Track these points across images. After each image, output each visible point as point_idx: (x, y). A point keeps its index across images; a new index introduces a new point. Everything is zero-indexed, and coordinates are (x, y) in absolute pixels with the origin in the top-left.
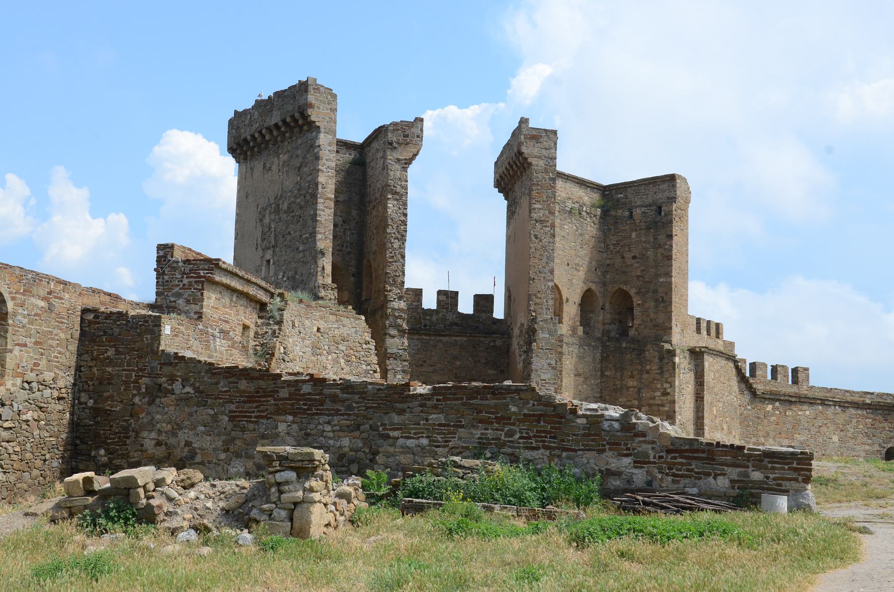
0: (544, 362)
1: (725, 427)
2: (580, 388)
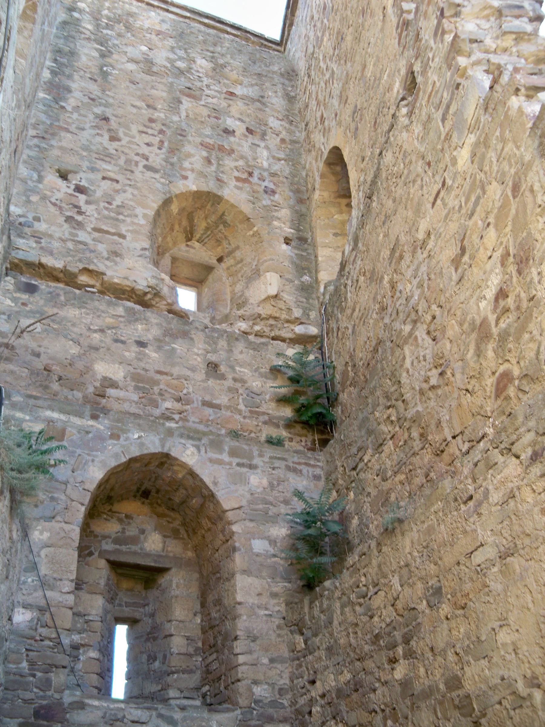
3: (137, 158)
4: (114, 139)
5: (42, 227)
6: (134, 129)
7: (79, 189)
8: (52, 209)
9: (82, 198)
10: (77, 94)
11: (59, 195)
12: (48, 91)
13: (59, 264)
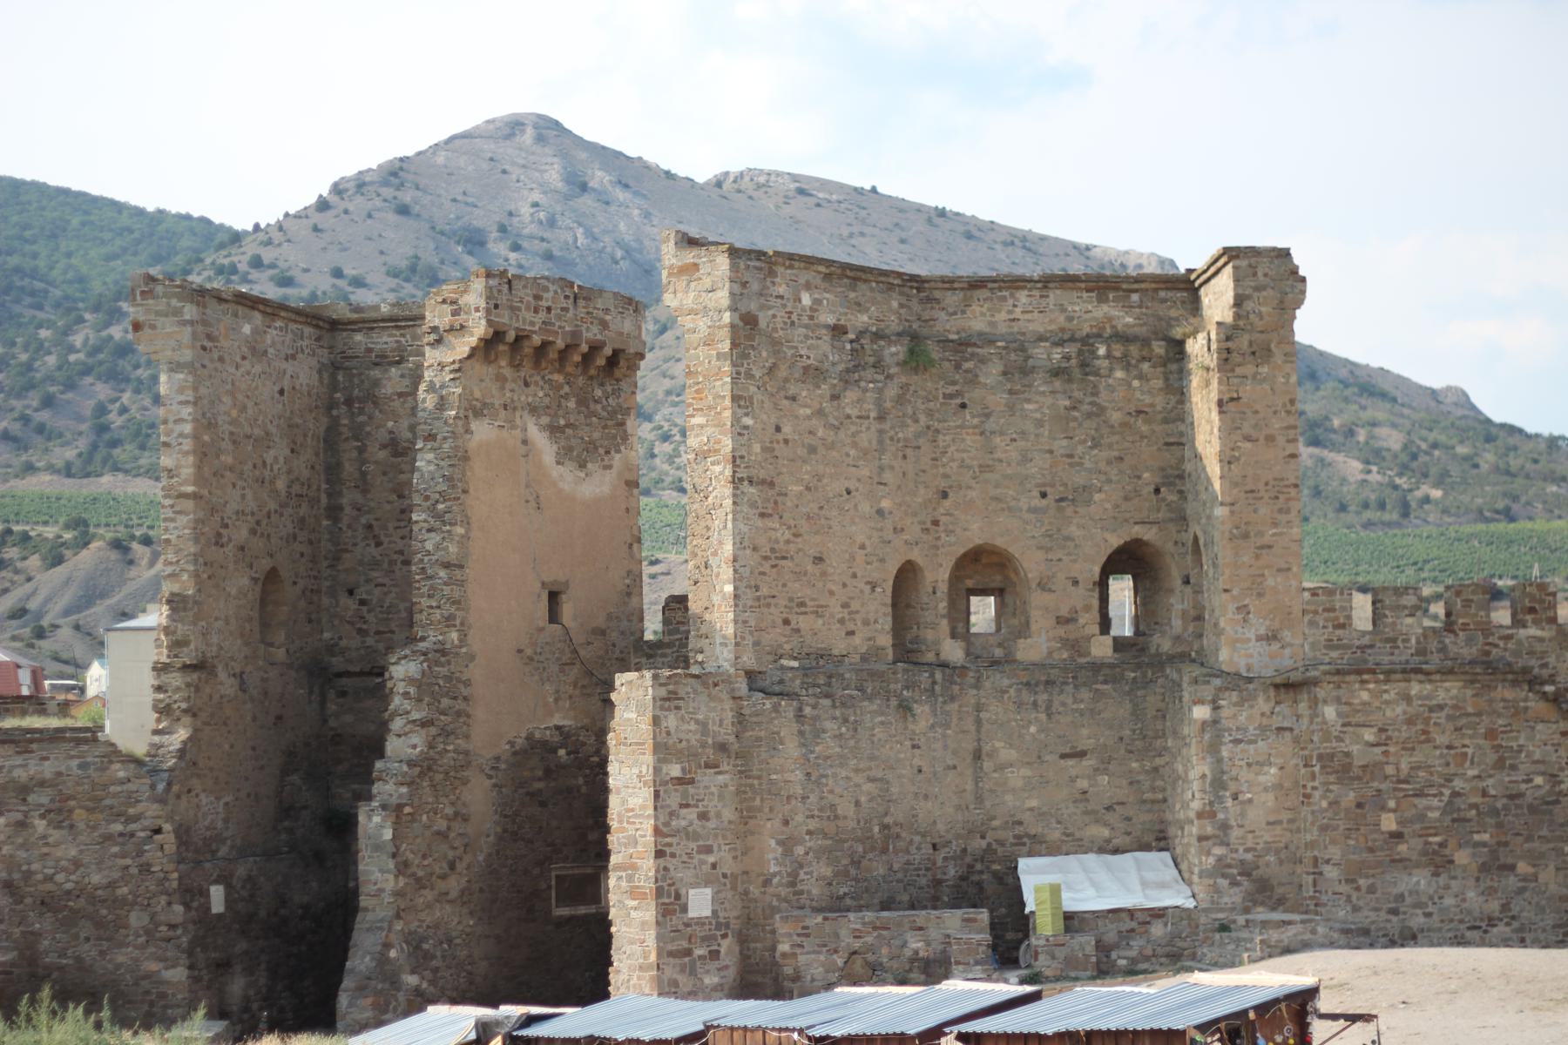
0: (625, 770)
1: (1462, 857)
2: (1083, 784)
3: (395, 557)
4: (378, 544)
5: (343, 643)
6: (391, 526)
7: (363, 602)
8: (347, 627)
9: (365, 608)
10: (348, 510)
11: (350, 613)
12: (328, 517)
13: (357, 669)
